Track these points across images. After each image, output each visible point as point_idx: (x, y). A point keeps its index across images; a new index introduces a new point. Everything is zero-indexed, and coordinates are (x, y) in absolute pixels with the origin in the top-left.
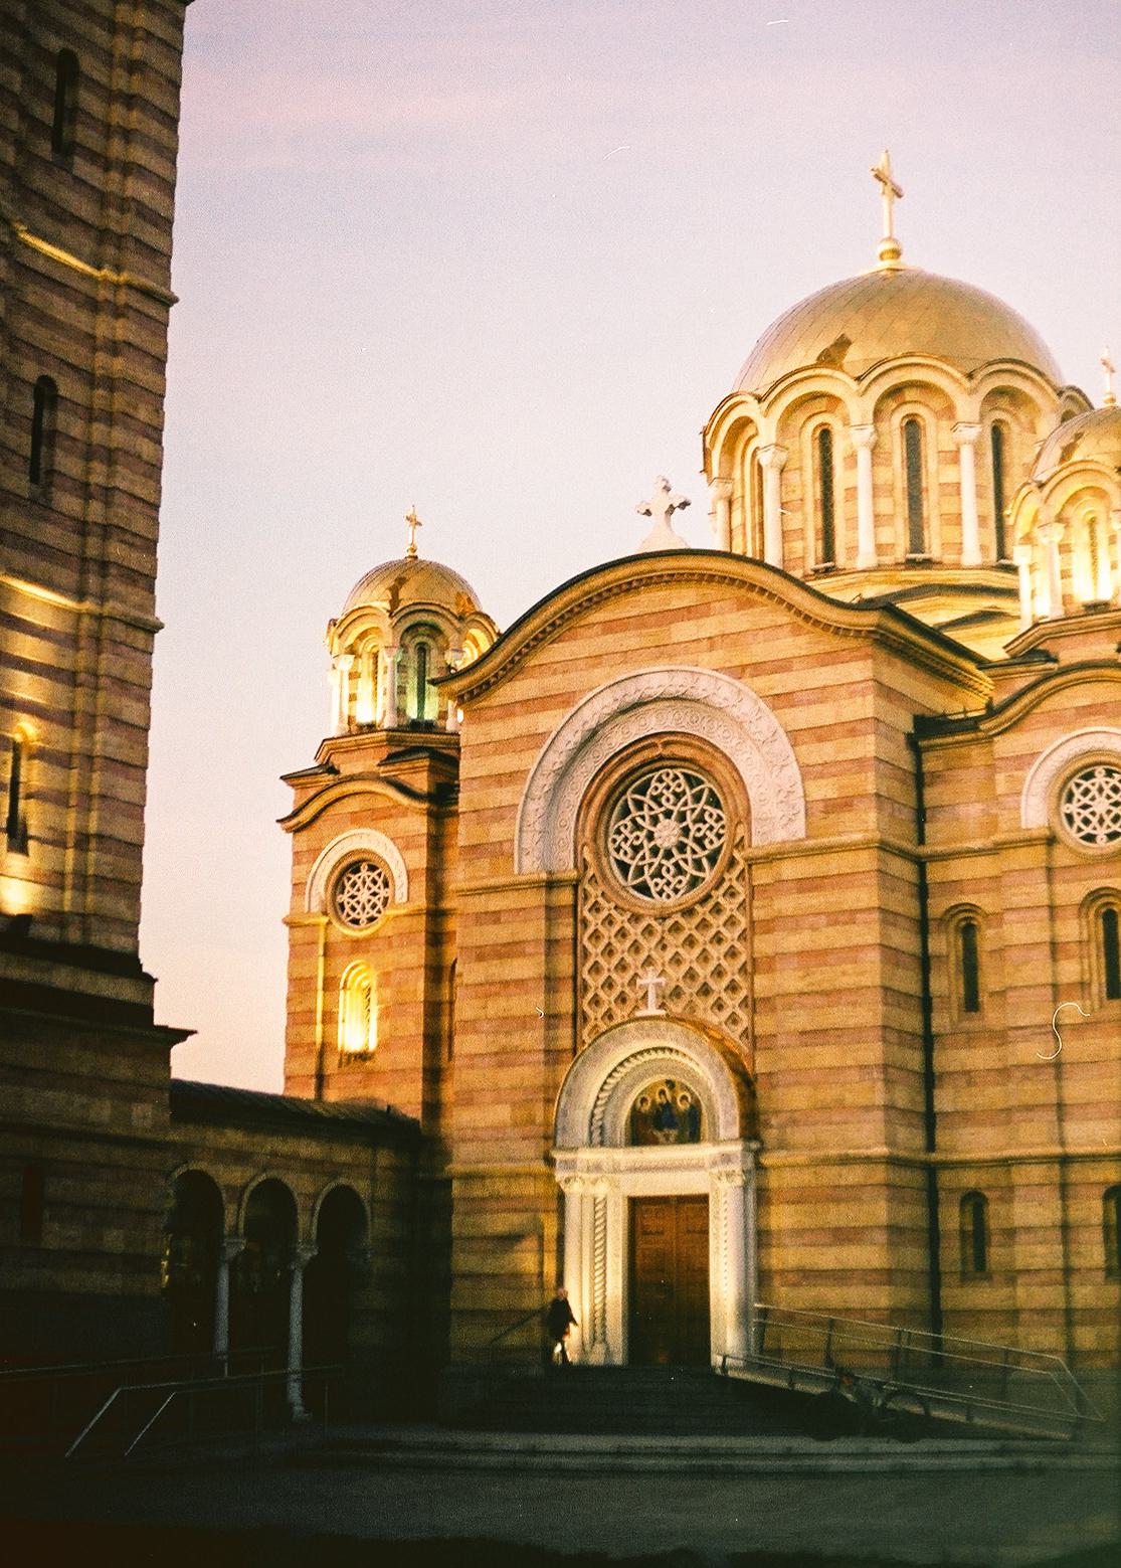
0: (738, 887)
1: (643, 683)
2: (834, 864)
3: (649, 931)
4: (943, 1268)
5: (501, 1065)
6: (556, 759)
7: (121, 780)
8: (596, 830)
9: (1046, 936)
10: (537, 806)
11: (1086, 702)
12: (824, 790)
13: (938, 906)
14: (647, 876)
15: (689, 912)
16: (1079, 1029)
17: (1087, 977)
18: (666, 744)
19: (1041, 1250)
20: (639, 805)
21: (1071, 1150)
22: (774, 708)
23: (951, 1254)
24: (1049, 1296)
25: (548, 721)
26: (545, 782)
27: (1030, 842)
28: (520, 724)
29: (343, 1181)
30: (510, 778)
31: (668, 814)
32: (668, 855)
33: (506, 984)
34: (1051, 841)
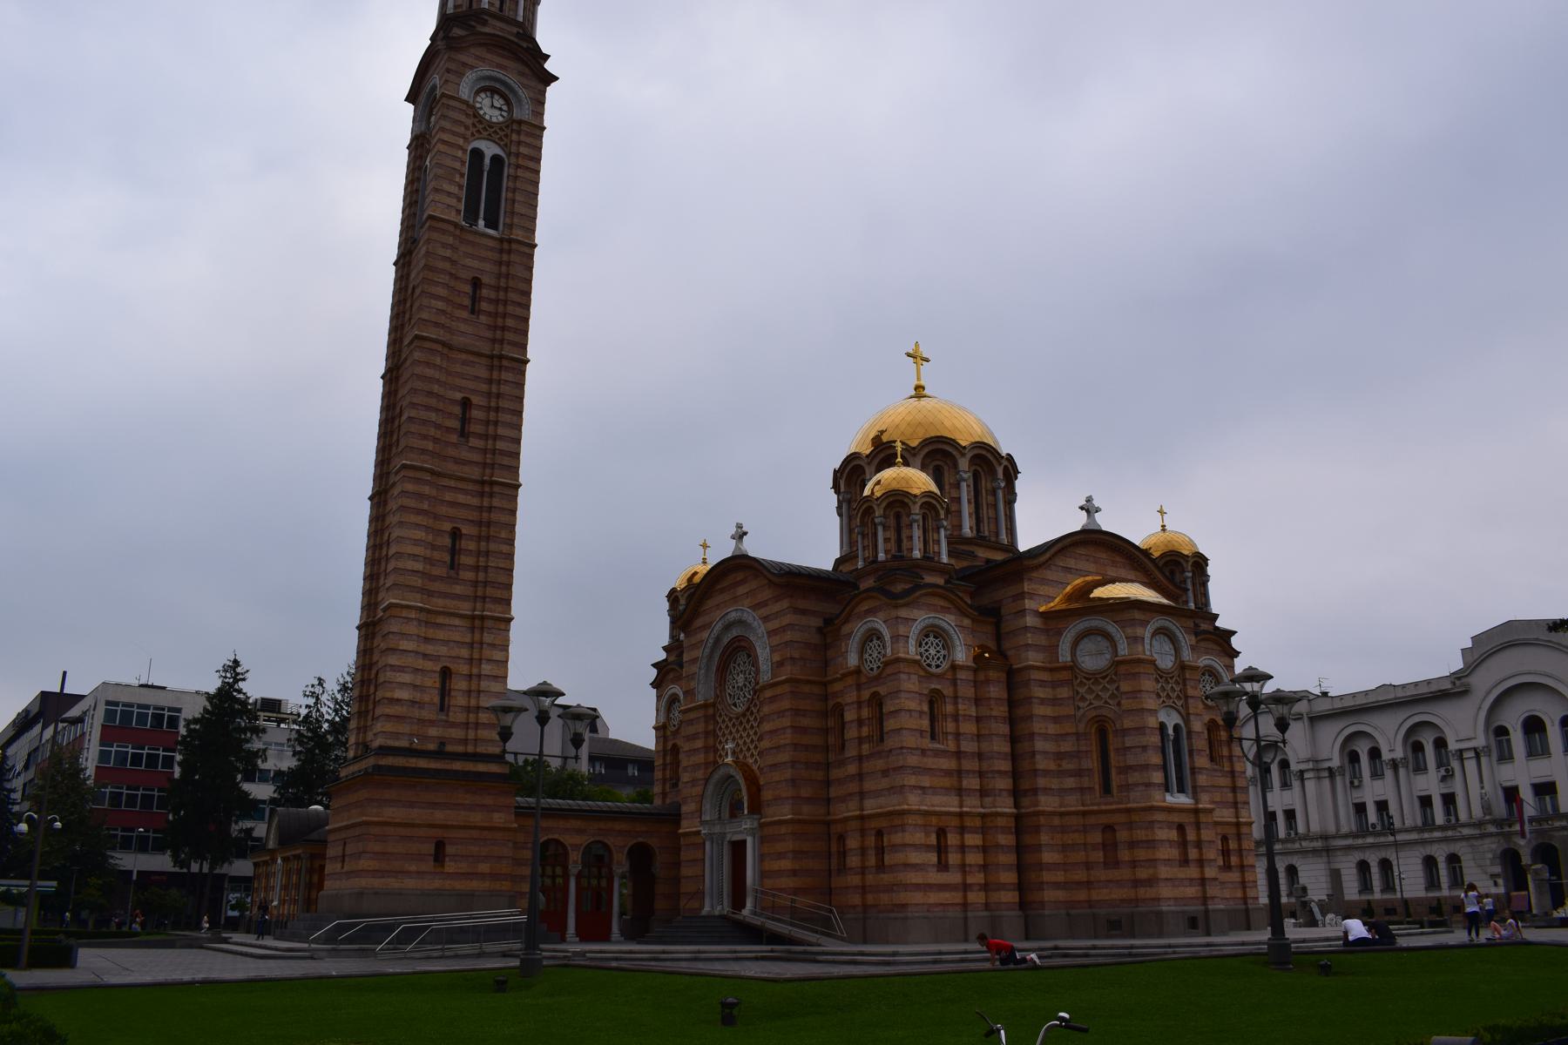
0: (758, 703)
1: (728, 617)
2: (778, 690)
3: (734, 725)
4: (832, 868)
5: (693, 786)
6: (707, 650)
7: (493, 683)
8: (720, 682)
9: (855, 717)
10: (703, 671)
11: (867, 608)
12: (777, 658)
13: (831, 703)
15: (744, 715)
16: (871, 756)
17: (871, 733)
18: (739, 641)
19: (854, 859)
20: (734, 667)
21: (865, 812)
22: (764, 622)
23: (834, 862)
24: (855, 880)
25: (705, 635)
26: (705, 661)
27: (850, 673)
28: (699, 637)
29: (640, 840)
30: (694, 661)
31: (741, 671)
32: (742, 690)
33: (694, 750)
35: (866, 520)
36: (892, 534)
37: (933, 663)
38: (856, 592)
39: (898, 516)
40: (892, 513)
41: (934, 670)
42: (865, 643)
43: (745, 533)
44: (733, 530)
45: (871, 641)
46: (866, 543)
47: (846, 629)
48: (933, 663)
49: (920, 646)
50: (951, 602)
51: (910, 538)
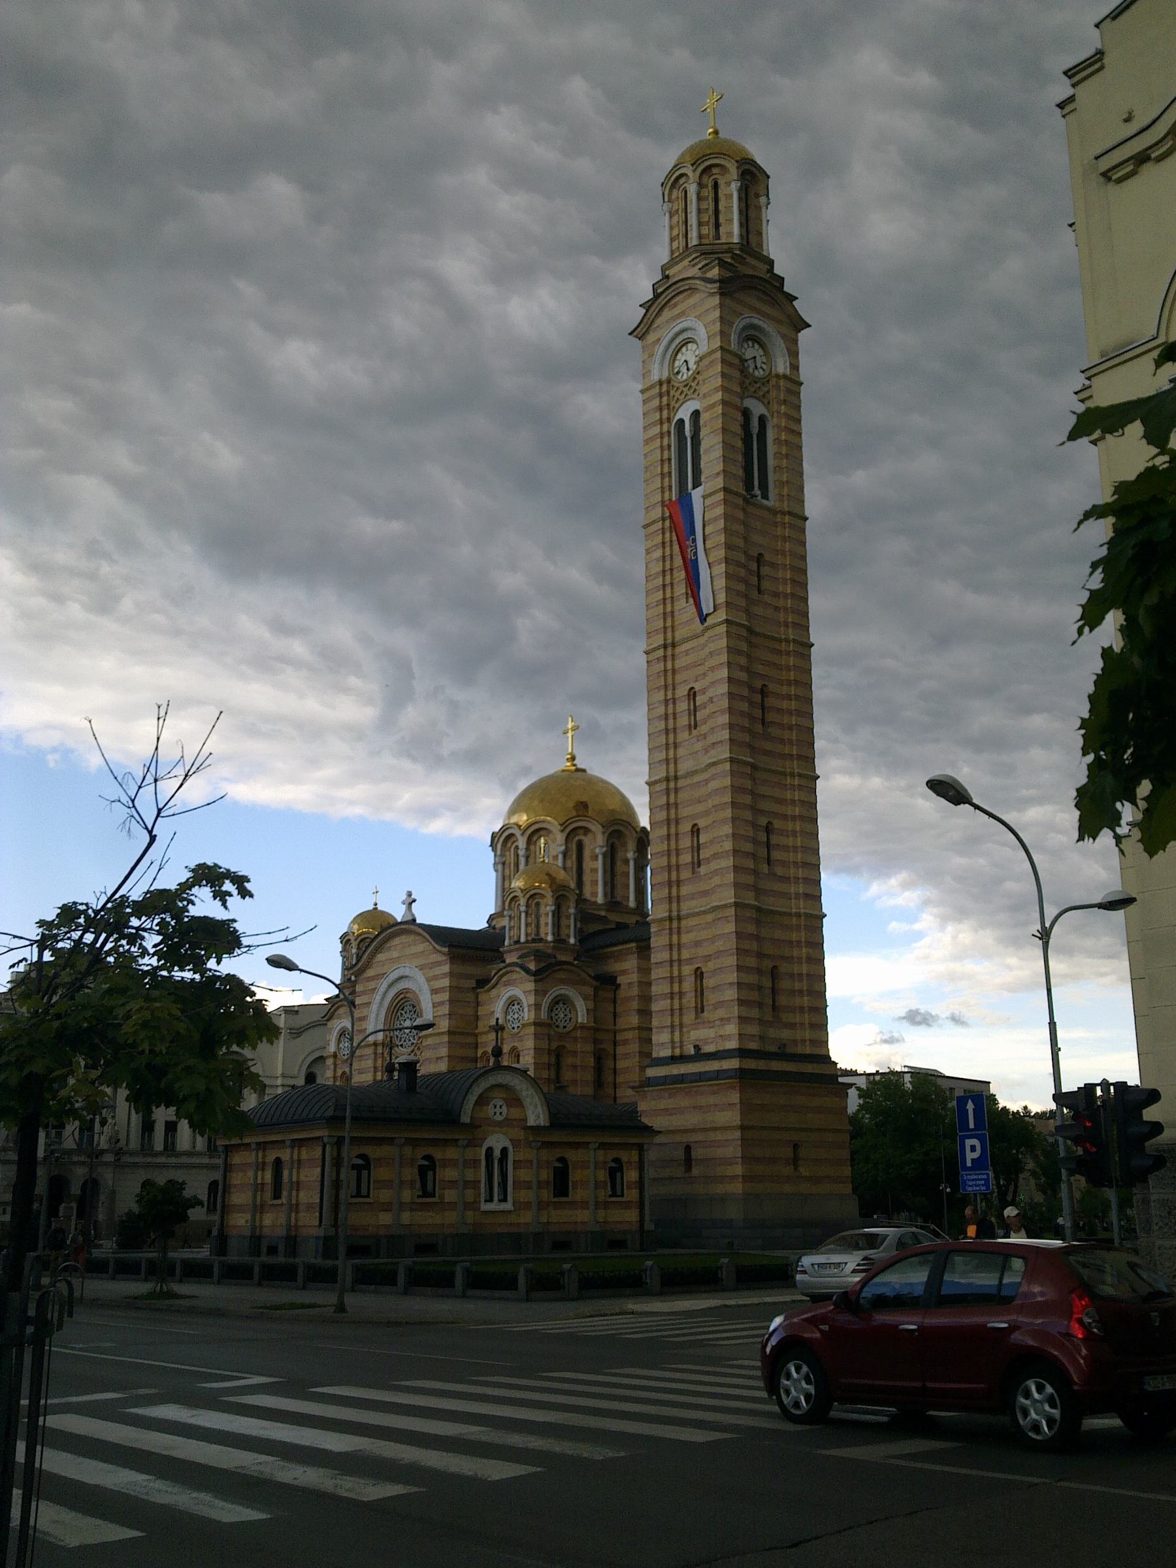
14: (403, 1040)
18: (407, 992)
20: (401, 1014)
35: (513, 905)
37: (561, 1025)
38: (503, 965)
39: (538, 904)
41: (561, 1030)
42: (507, 1008)
43: (414, 901)
44: (404, 897)
45: (513, 1005)
46: (512, 924)
47: (494, 992)
48: (561, 1025)
49: (552, 1011)
51: (547, 924)
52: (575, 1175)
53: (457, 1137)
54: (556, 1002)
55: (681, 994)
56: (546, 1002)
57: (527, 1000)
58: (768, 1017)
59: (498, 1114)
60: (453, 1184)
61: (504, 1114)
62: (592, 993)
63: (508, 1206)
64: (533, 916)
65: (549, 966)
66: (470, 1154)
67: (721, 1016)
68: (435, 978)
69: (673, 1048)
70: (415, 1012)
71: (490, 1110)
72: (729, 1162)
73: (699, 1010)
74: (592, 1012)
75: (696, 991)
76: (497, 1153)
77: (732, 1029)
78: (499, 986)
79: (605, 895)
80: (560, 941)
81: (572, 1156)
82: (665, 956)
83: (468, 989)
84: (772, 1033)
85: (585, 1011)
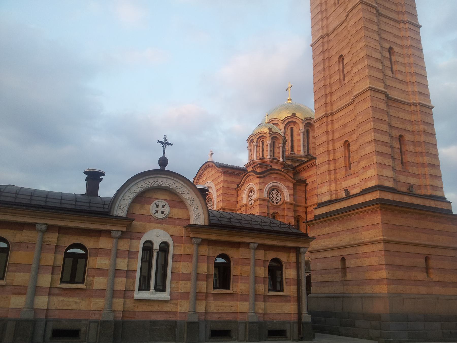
34: (246, 205)
36: (260, 149)
37: (275, 201)
39: (263, 142)
40: (261, 141)
41: (275, 204)
47: (243, 188)
48: (275, 201)
49: (270, 194)
50: (284, 176)
51: (267, 151)
52: (235, 271)
53: (108, 228)
54: (272, 189)
55: (335, 160)
56: (266, 189)
57: (256, 188)
58: (399, 167)
59: (160, 212)
60: (102, 272)
61: (166, 212)
62: (293, 186)
63: (165, 295)
64: (260, 148)
65: (268, 170)
66: (124, 245)
67: (363, 166)
68: (218, 184)
69: (331, 195)
70: (212, 203)
71: (152, 209)
72: (377, 268)
73: (348, 168)
74: (294, 195)
75: (345, 156)
76: (156, 247)
77: (372, 172)
78: (244, 184)
79: (304, 151)
80: (274, 160)
81: (232, 253)
82: (324, 138)
83: (233, 188)
84: (402, 178)
85: (288, 195)
